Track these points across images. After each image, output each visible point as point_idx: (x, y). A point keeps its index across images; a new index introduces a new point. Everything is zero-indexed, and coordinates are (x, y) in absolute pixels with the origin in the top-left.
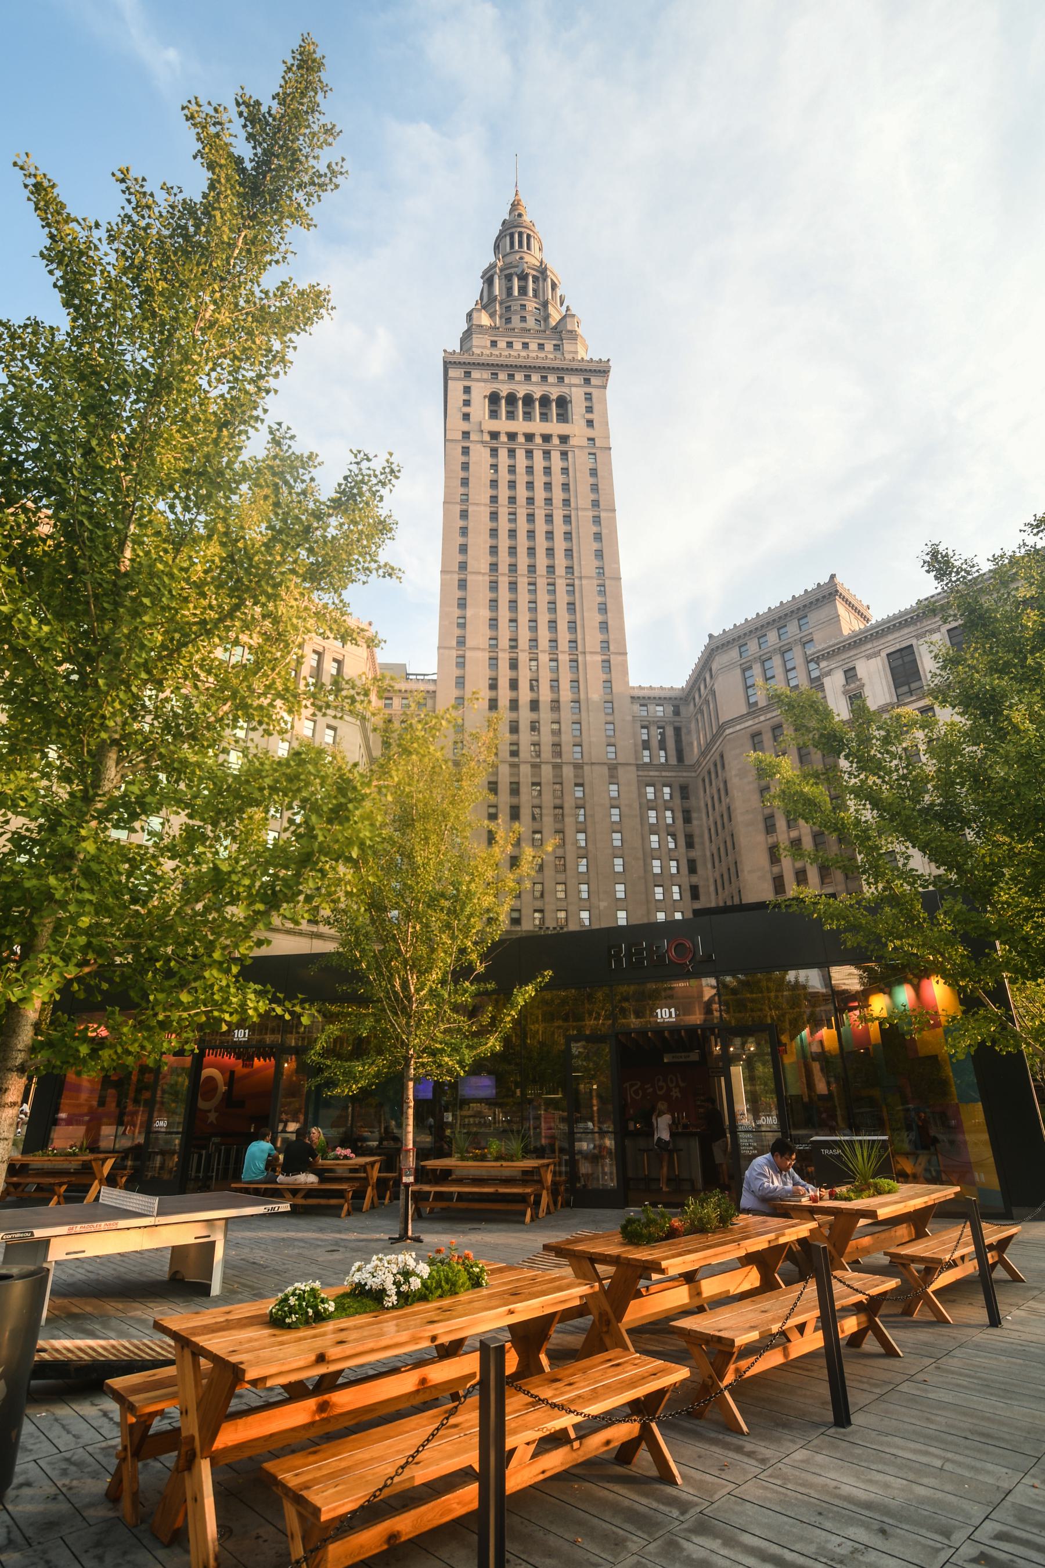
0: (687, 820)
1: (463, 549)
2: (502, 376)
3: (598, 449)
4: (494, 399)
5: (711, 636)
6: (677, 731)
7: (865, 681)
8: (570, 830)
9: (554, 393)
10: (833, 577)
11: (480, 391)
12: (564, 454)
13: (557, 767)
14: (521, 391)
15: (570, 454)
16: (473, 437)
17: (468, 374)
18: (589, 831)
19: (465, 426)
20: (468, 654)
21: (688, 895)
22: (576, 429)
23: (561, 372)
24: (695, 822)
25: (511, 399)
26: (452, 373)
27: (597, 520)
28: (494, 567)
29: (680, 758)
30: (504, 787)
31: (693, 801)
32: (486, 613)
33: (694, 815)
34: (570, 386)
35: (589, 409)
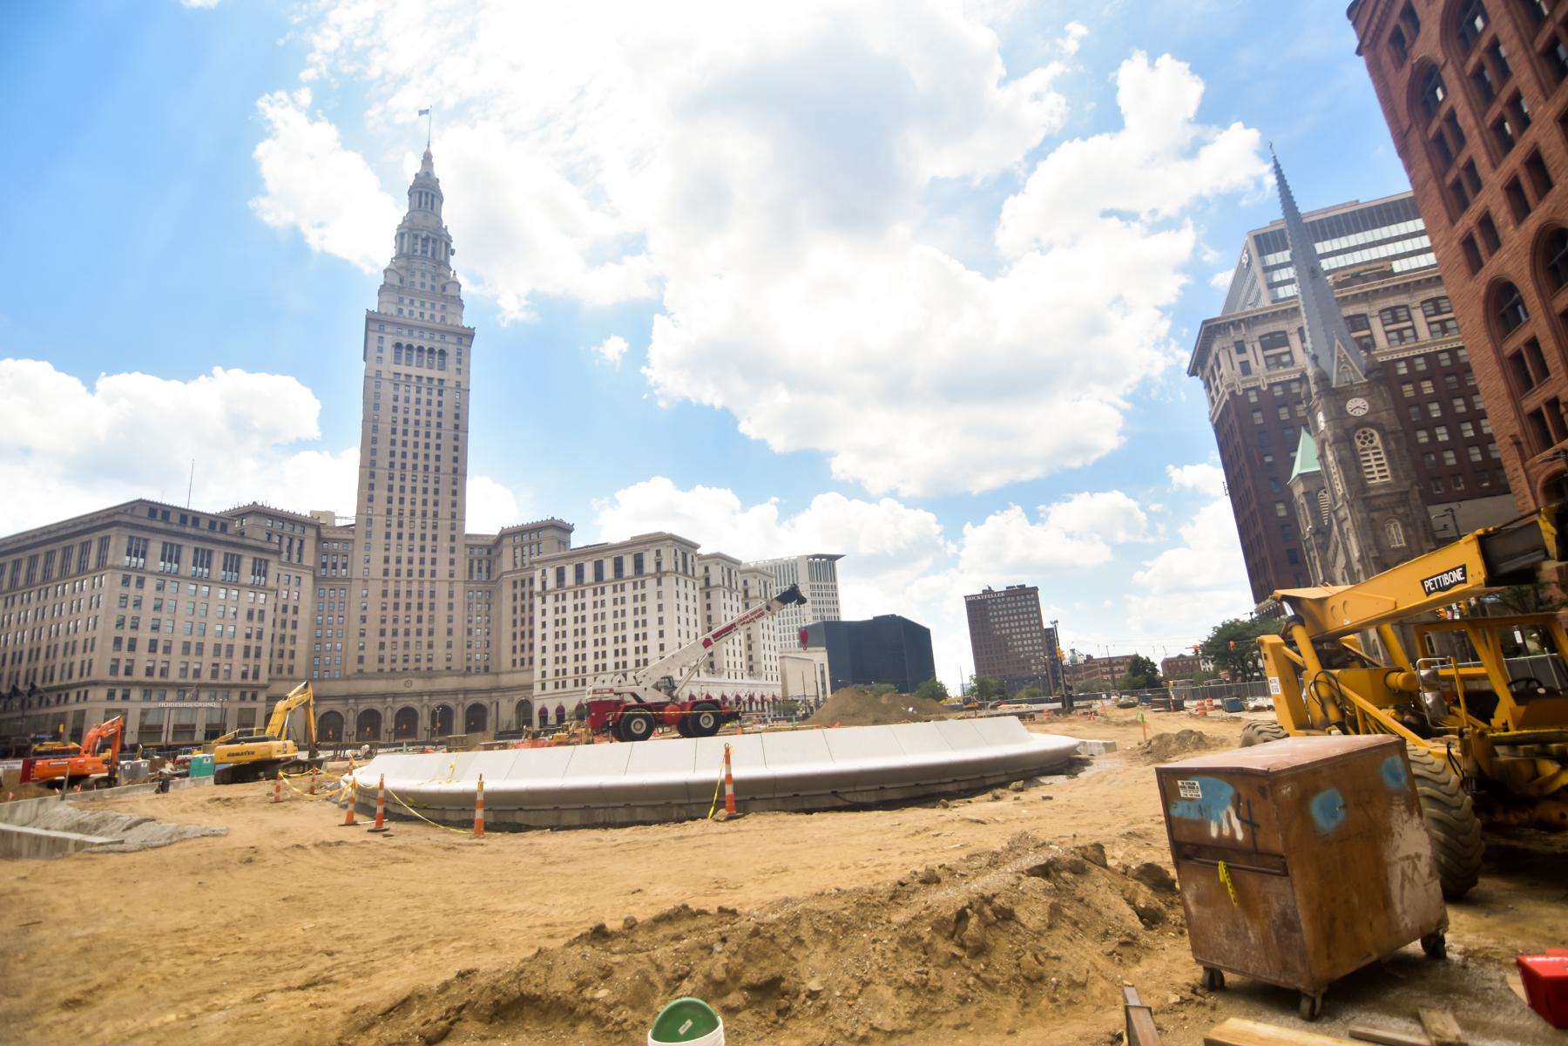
1: (374, 452)
2: (405, 332)
3: (462, 389)
4: (398, 346)
12: (440, 393)
14: (416, 344)
16: (384, 375)
17: (381, 329)
19: (379, 367)
22: (449, 375)
23: (444, 333)
25: (410, 347)
27: (456, 439)
28: (392, 465)
30: (391, 593)
32: (386, 493)
35: (459, 362)
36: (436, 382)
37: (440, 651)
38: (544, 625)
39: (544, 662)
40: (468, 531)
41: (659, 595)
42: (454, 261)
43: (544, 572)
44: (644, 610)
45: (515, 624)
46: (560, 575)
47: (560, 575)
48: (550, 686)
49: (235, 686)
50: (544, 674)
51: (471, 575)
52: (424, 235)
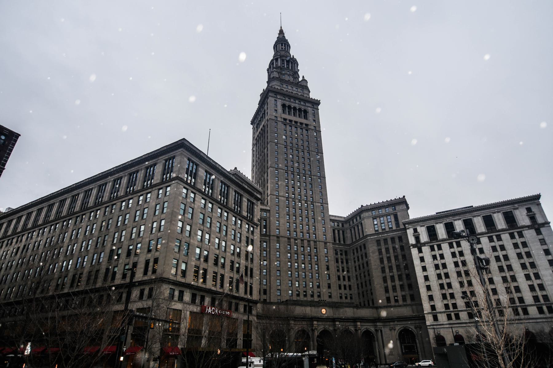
0: (347, 263)
4: (284, 106)
5: (362, 206)
6: (343, 232)
7: (420, 233)
8: (313, 264)
9: (303, 108)
10: (404, 196)
11: (279, 103)
12: (307, 130)
13: (309, 241)
14: (293, 105)
15: (309, 131)
16: (279, 119)
18: (319, 264)
20: (280, 198)
21: (348, 288)
24: (350, 264)
25: (289, 107)
26: (270, 94)
29: (344, 242)
31: (349, 257)
32: (284, 184)
33: (349, 261)
34: (308, 107)
36: (304, 126)
37: (324, 290)
38: (424, 269)
39: (431, 298)
40: (331, 213)
41: (543, 242)
42: (301, 74)
43: (415, 230)
44: (529, 255)
45: (383, 271)
46: (432, 232)
47: (432, 232)
48: (442, 318)
49: (242, 299)
50: (433, 308)
51: (335, 240)
52: (288, 59)
